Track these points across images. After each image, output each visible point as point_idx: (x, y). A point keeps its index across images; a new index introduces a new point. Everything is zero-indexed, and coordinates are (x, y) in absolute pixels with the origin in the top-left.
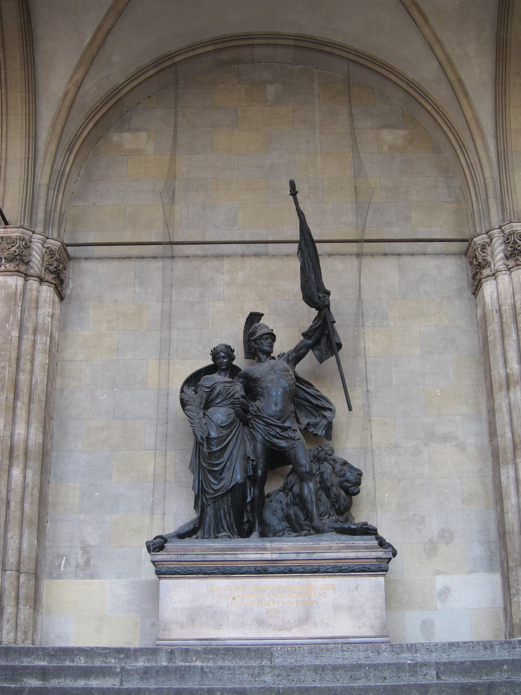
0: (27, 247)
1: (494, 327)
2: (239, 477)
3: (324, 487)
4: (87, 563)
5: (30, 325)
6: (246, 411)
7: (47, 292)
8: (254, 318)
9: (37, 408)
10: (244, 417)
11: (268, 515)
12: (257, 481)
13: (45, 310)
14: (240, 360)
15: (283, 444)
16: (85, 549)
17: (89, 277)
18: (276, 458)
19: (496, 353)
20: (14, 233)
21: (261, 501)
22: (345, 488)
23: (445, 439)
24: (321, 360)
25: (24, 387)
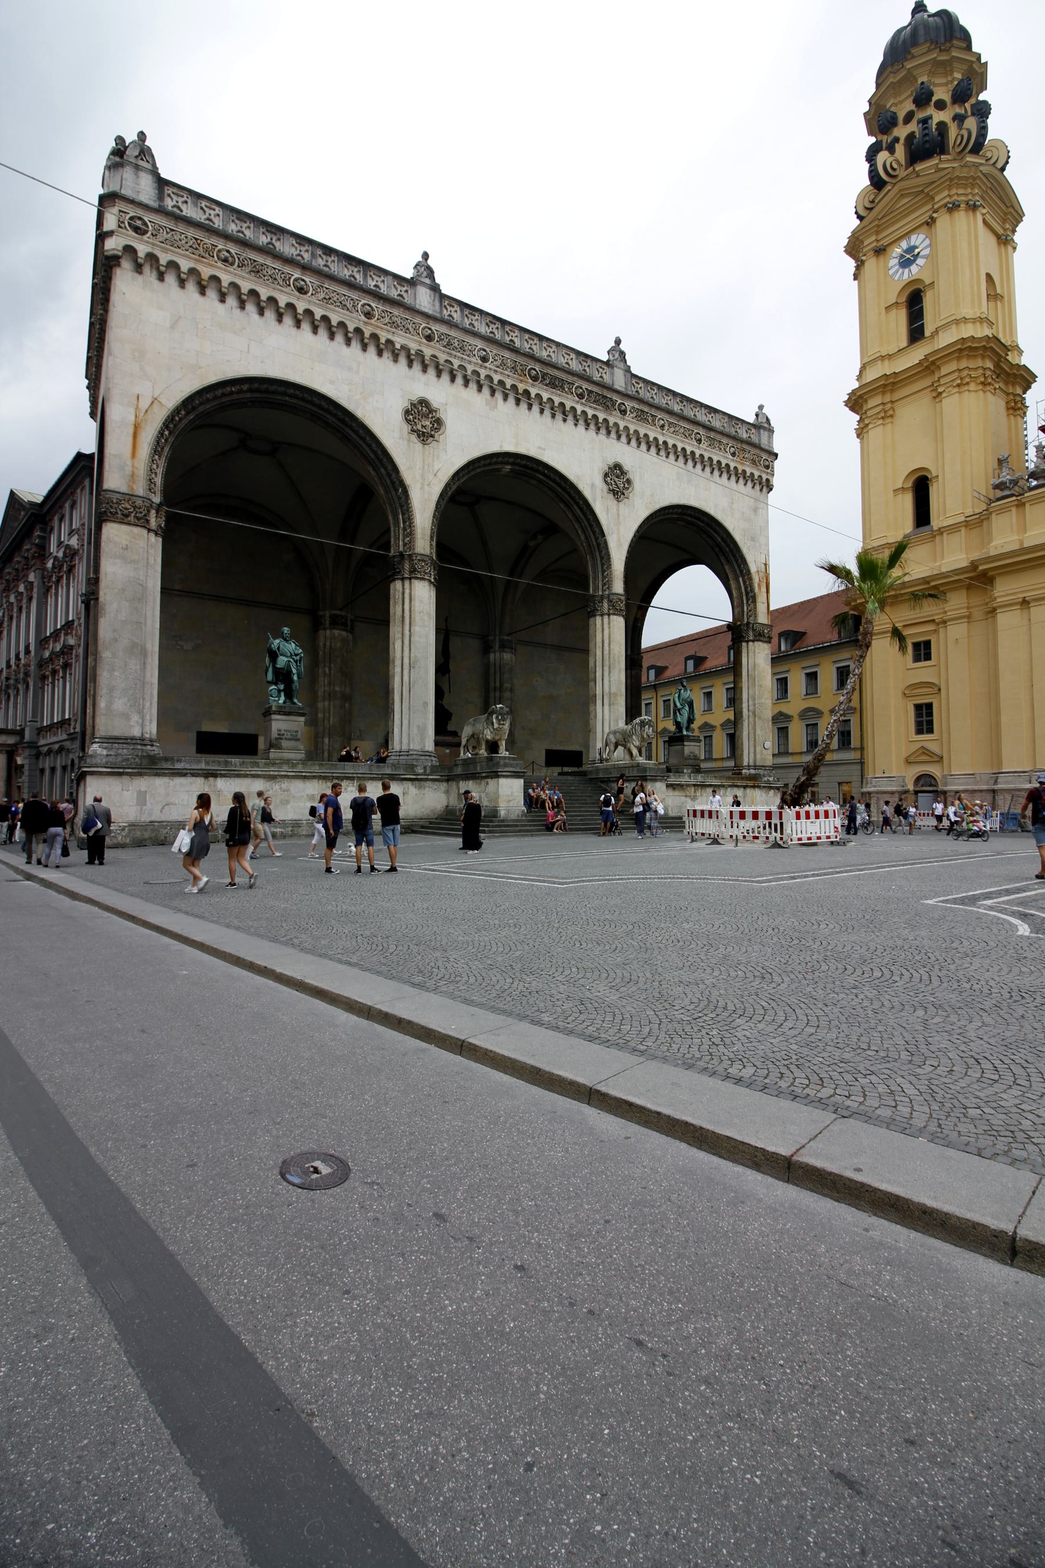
1: (492, 670)
7: (350, 636)
16: (360, 731)
19: (492, 679)
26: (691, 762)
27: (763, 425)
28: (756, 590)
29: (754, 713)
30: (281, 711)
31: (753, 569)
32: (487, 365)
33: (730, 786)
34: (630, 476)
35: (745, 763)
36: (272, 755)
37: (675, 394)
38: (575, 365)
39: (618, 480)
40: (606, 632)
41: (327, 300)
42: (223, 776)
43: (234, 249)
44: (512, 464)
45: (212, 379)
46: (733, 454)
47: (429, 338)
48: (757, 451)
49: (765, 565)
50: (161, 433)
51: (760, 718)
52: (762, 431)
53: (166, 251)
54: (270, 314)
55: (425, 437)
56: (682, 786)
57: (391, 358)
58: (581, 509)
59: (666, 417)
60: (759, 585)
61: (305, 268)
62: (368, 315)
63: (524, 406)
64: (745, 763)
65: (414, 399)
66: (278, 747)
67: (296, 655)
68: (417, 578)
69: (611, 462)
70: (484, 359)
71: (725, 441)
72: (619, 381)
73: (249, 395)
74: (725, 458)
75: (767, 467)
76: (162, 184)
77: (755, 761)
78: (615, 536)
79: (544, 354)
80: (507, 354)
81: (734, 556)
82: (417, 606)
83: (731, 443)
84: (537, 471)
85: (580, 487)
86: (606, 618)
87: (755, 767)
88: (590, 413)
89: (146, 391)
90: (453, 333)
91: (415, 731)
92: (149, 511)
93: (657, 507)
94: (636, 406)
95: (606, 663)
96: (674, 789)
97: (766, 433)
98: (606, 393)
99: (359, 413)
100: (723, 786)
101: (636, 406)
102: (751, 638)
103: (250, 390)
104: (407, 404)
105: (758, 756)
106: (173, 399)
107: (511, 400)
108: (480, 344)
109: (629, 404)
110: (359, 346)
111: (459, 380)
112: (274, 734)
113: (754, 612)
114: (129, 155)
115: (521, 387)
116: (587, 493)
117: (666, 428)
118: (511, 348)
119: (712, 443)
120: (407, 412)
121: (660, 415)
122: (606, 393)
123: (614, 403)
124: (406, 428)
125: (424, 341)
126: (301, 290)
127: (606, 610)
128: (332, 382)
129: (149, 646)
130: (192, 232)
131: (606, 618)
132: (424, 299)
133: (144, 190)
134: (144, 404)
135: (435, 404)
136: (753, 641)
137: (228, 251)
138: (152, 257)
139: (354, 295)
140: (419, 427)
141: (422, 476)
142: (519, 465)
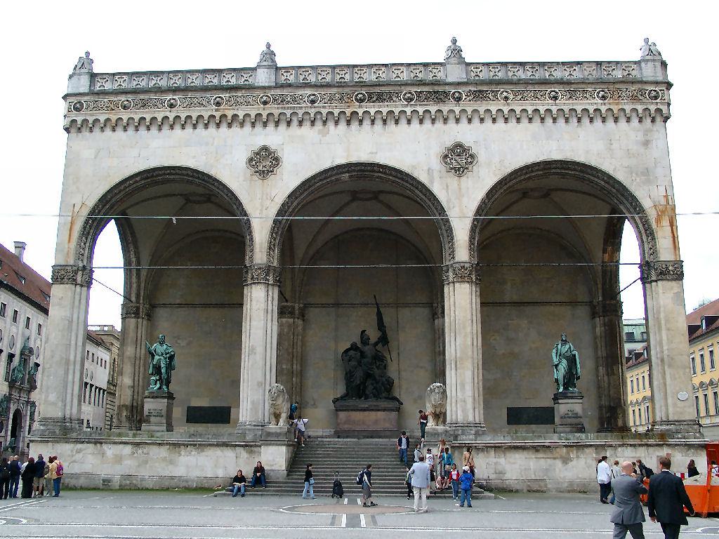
0: (293, 308)
2: (358, 382)
3: (383, 384)
4: (314, 404)
5: (296, 334)
6: (361, 362)
7: (300, 322)
8: (363, 332)
9: (299, 359)
10: (360, 363)
11: (367, 392)
12: (364, 383)
13: (300, 328)
14: (359, 345)
15: (372, 372)
16: (313, 399)
17: (313, 313)
18: (368, 376)
20: (289, 304)
21: (365, 387)
22: (389, 385)
23: (422, 367)
24: (383, 346)
25: (295, 354)
26: (569, 421)
27: (653, 55)
28: (654, 226)
29: (662, 360)
30: (154, 396)
31: (646, 203)
32: (316, 105)
33: (620, 446)
34: (474, 151)
35: (658, 419)
36: (143, 428)
37: (522, 64)
38: (405, 76)
39: (459, 159)
40: (452, 299)
42: (106, 443)
43: (130, 97)
44: (348, 172)
45: (117, 180)
46: (604, 98)
47: (265, 103)
48: (636, 87)
49: (666, 196)
50: (86, 222)
51: (670, 366)
52: (643, 64)
53: (92, 115)
54: (154, 130)
55: (264, 174)
56: (549, 447)
57: (239, 126)
58: (421, 192)
59: (508, 87)
60: (658, 220)
61: (176, 90)
62: (218, 104)
63: (355, 125)
64: (658, 419)
65: (256, 149)
66: (148, 421)
67: (166, 354)
68: (254, 283)
69: (449, 144)
70: (313, 102)
72: (455, 74)
73: (143, 182)
74: (592, 104)
75: (656, 98)
76: (93, 76)
77: (668, 416)
78: (457, 209)
79: (373, 78)
80: (334, 90)
81: (623, 195)
82: (254, 303)
84: (373, 171)
85: (415, 175)
86: (452, 285)
87: (668, 422)
88: (421, 110)
89: (77, 200)
90: (285, 92)
91: (249, 406)
92: (76, 274)
93: (509, 170)
95: (453, 328)
96: (537, 451)
97: (650, 64)
98: (436, 88)
99: (213, 172)
100: (611, 446)
101: (473, 89)
102: (654, 278)
103: (141, 180)
104: (249, 155)
105: (671, 410)
106: (92, 201)
107: (343, 125)
108: (308, 92)
110: (215, 126)
111: (295, 122)
112: (146, 413)
113: (654, 252)
114: (85, 63)
115: (348, 112)
116: (423, 178)
117: (511, 96)
118: (341, 85)
119: (572, 95)
120: (251, 160)
122: (436, 88)
123: (446, 94)
124: (250, 171)
125: (262, 106)
126: (172, 106)
127: (451, 279)
128: (194, 157)
129: (72, 358)
131: (452, 285)
132: (263, 78)
133: (83, 85)
134: (76, 209)
135: (273, 148)
136: (656, 281)
137: (128, 101)
138: (85, 121)
140: (260, 168)
141: (262, 206)
142: (354, 171)
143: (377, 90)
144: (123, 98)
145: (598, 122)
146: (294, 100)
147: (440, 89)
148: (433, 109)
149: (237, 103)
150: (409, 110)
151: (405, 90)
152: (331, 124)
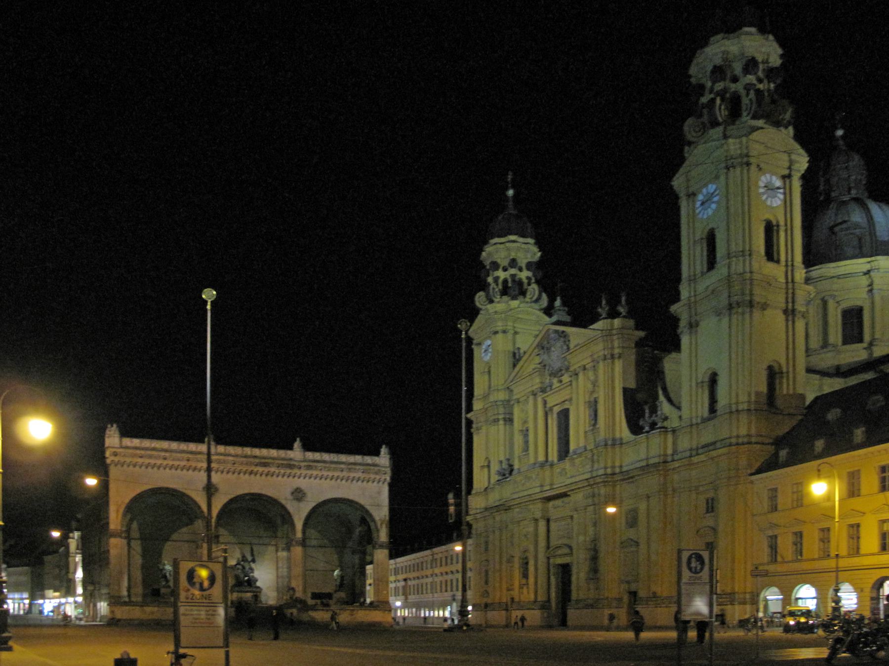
41: (173, 460)
43: (143, 452)
62: (188, 460)
71: (358, 467)
83: (361, 467)
94: (306, 464)
101: (306, 464)
108: (231, 458)
109: (303, 464)
115: (250, 469)
119: (350, 470)
121: (319, 465)
123: (294, 465)
126: (165, 459)
130: (130, 451)
139: (183, 455)
143: (263, 461)
144: (138, 452)
145: (360, 483)
146: (224, 462)
147: (292, 463)
148: (288, 471)
149: (198, 461)
150: (277, 471)
151: (277, 462)
152: (242, 474)
